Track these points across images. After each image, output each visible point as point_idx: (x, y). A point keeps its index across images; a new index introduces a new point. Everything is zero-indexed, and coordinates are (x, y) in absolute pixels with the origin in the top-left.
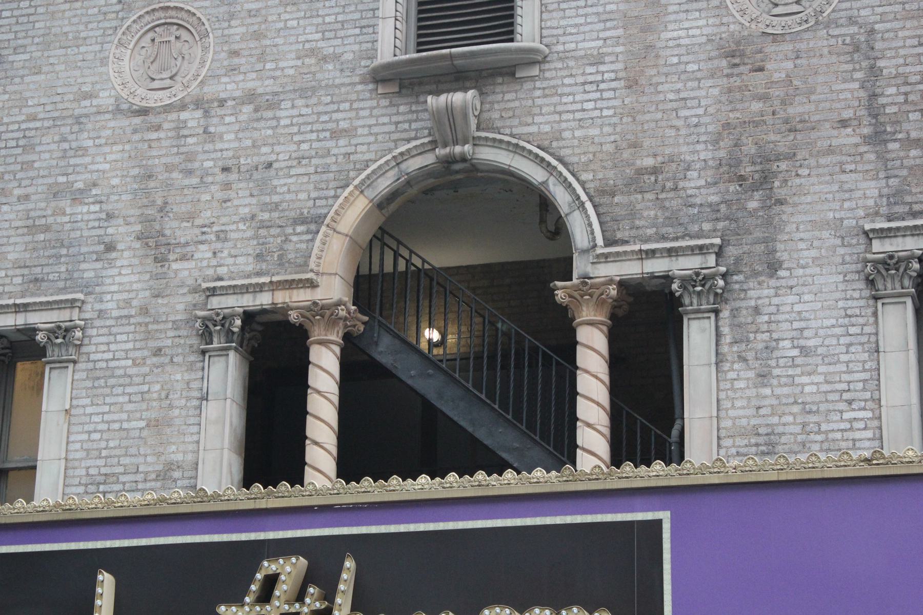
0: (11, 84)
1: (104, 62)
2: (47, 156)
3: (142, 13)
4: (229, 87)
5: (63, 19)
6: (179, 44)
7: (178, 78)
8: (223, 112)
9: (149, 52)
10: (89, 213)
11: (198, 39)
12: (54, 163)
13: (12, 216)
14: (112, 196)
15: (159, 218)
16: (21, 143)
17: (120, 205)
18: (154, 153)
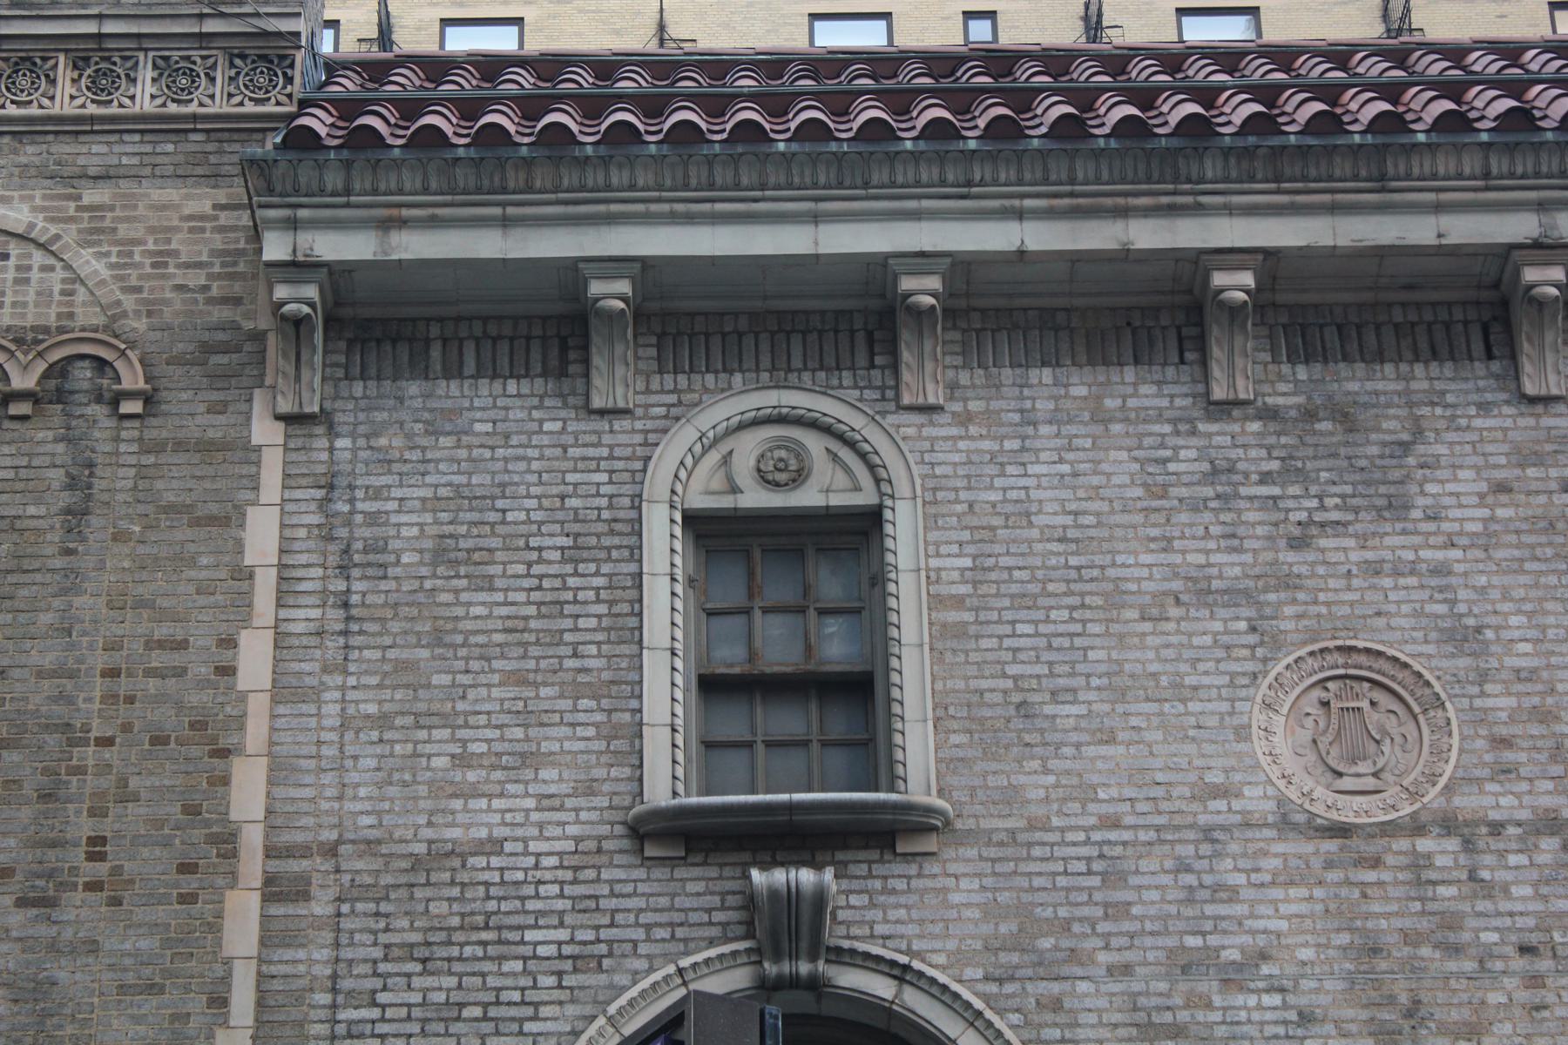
0: (1057, 756)
1: (1242, 733)
2: (1154, 895)
3: (1302, 652)
4: (1503, 801)
5: (1144, 648)
6: (1376, 716)
7: (1386, 775)
8: (1501, 846)
9: (1322, 724)
10: (1259, 1007)
11: (1417, 709)
12: (1173, 909)
13: (1102, 1003)
14: (1303, 982)
15: (1407, 1029)
16: (1097, 866)
17: (1324, 999)
18: (1376, 908)
